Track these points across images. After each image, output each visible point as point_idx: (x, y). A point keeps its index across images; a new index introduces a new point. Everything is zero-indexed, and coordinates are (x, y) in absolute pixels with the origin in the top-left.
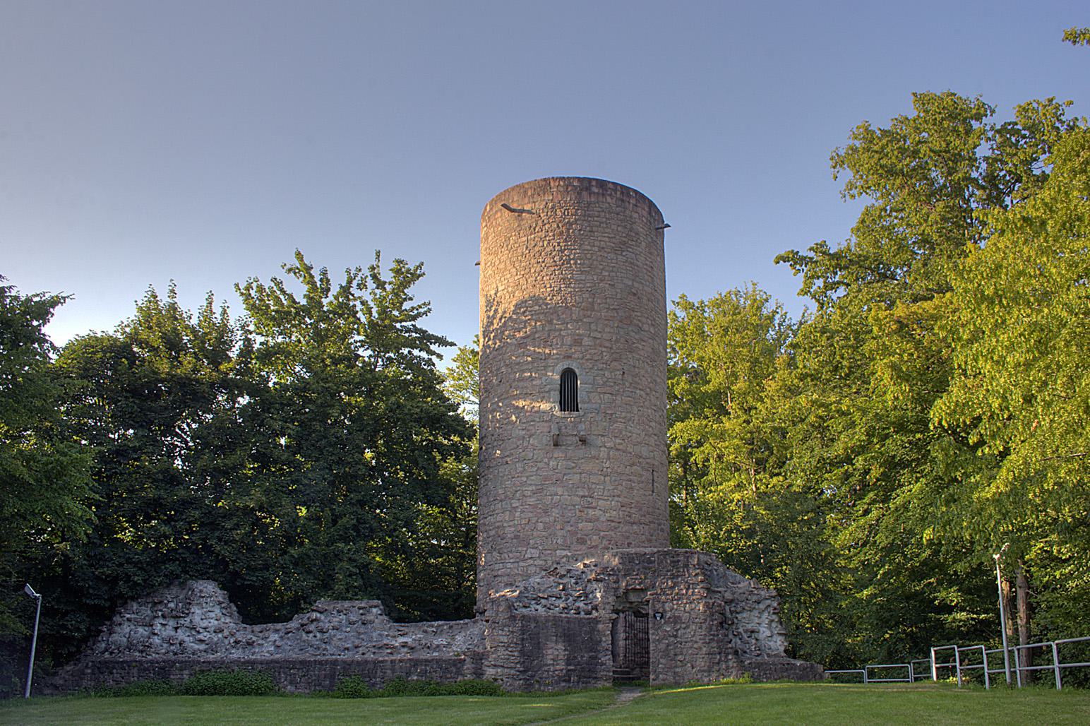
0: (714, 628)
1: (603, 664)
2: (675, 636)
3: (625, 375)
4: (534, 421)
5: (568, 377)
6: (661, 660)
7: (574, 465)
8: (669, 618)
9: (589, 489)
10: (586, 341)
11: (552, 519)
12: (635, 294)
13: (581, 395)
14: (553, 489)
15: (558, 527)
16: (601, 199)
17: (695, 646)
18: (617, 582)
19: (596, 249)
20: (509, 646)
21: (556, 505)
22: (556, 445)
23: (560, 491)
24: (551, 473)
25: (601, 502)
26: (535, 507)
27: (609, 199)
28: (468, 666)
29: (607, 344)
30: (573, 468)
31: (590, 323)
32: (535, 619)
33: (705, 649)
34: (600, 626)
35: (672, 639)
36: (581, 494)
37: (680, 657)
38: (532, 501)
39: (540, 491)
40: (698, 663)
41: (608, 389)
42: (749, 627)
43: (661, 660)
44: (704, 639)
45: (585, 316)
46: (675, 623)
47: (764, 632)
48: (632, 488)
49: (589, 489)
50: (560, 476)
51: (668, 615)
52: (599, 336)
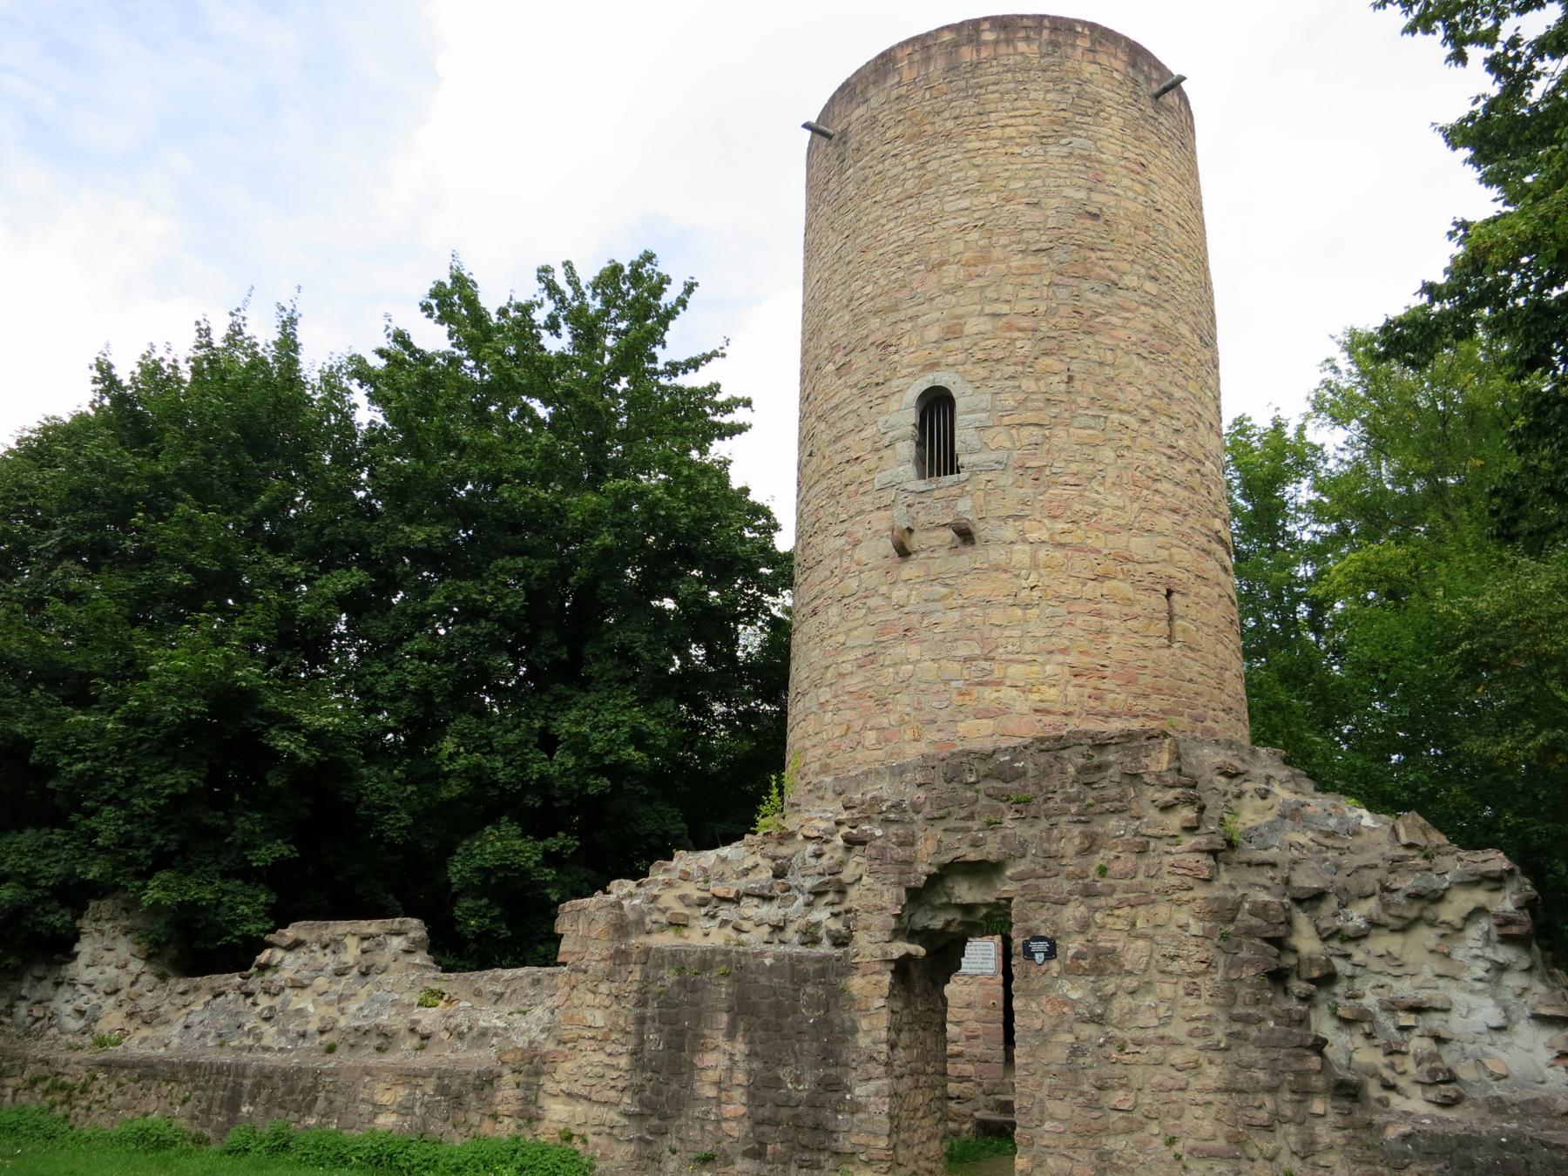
0: (1244, 992)
1: (856, 1107)
2: (1098, 1020)
3: (1077, 384)
4: (862, 512)
5: (937, 407)
6: (1051, 1105)
7: (945, 591)
8: (1079, 956)
9: (983, 640)
10: (973, 326)
11: (894, 718)
12: (1095, 216)
13: (964, 435)
14: (899, 651)
15: (908, 736)
16: (1002, 49)
17: (1177, 1056)
18: (907, 842)
19: (994, 143)
20: (606, 1039)
21: (905, 683)
22: (903, 552)
23: (913, 651)
24: (895, 615)
25: (1014, 670)
26: (859, 695)
27: (1022, 47)
28: (507, 1093)
29: (1025, 323)
30: (944, 597)
31: (983, 288)
32: (675, 958)
33: (1213, 1071)
34: (856, 984)
35: (1089, 1030)
36: (963, 652)
37: (1117, 1097)
38: (853, 683)
39: (871, 658)
40: (1188, 1121)
41: (1030, 417)
42: (1405, 989)
43: (1051, 1105)
44: (1207, 1033)
45: (970, 277)
46: (1098, 971)
47: (1472, 1012)
48: (1103, 632)
49: (983, 640)
50: (914, 619)
51: (1073, 945)
52: (1005, 309)
